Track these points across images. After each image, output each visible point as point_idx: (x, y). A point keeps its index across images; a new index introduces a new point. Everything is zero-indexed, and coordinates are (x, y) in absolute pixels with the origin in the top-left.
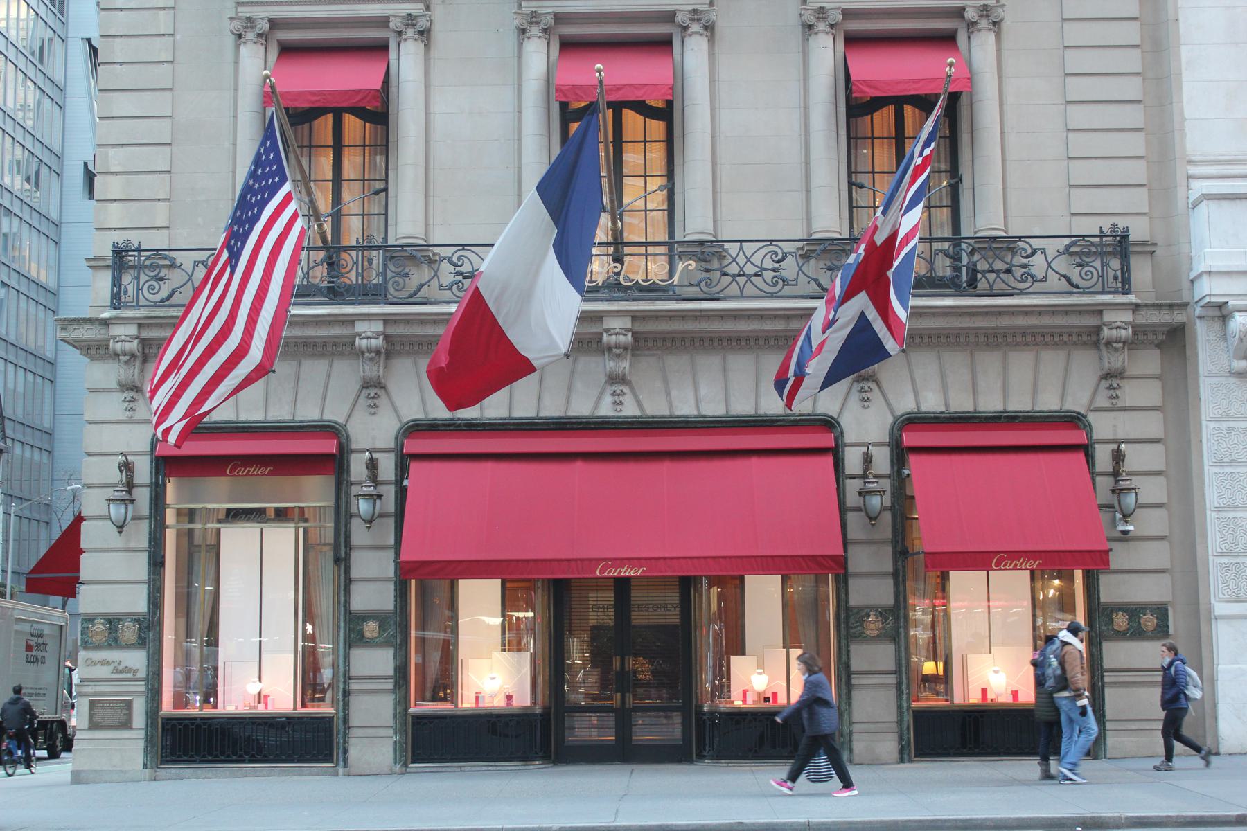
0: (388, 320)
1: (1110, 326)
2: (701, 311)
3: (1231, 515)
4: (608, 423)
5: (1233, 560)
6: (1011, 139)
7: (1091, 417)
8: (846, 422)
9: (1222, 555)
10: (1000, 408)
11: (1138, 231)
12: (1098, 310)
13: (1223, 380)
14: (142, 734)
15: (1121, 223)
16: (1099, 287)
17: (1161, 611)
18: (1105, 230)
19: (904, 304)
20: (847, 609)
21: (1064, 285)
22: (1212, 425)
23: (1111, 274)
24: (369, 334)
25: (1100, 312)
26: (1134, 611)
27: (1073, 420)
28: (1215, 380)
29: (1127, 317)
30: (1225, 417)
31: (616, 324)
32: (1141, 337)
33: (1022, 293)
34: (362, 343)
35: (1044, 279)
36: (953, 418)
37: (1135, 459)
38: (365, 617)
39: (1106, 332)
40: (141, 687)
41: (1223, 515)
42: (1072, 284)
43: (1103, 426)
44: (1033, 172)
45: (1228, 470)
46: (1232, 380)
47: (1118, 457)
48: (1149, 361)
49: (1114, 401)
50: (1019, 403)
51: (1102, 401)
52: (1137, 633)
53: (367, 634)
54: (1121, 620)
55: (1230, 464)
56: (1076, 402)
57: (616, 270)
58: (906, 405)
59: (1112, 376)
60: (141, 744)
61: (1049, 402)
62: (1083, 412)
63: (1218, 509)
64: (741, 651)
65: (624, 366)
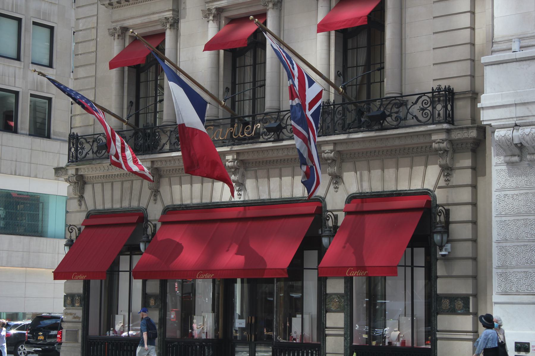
1: (434, 141)
2: (261, 148)
3: (504, 244)
4: (235, 204)
5: (504, 271)
7: (437, 192)
8: (328, 200)
9: (498, 267)
10: (394, 189)
11: (460, 85)
12: (429, 133)
14: (80, 344)
15: (444, 84)
16: (431, 121)
17: (465, 299)
18: (435, 89)
20: (146, 294)
21: (414, 121)
22: (497, 193)
23: (437, 112)
24: (438, 141)
25: (430, 135)
26: (452, 298)
29: (443, 136)
31: (229, 157)
35: (405, 119)
36: (373, 195)
37: (460, 214)
38: (151, 296)
39: (435, 145)
40: (80, 326)
41: (501, 244)
42: (419, 121)
43: (441, 197)
44: (419, 57)
45: (504, 219)
47: (447, 212)
49: (447, 183)
51: (442, 183)
52: (453, 311)
53: (151, 305)
54: (446, 303)
57: (232, 131)
58: (353, 189)
60: (79, 349)
62: (432, 189)
63: (498, 242)
64: (117, 314)
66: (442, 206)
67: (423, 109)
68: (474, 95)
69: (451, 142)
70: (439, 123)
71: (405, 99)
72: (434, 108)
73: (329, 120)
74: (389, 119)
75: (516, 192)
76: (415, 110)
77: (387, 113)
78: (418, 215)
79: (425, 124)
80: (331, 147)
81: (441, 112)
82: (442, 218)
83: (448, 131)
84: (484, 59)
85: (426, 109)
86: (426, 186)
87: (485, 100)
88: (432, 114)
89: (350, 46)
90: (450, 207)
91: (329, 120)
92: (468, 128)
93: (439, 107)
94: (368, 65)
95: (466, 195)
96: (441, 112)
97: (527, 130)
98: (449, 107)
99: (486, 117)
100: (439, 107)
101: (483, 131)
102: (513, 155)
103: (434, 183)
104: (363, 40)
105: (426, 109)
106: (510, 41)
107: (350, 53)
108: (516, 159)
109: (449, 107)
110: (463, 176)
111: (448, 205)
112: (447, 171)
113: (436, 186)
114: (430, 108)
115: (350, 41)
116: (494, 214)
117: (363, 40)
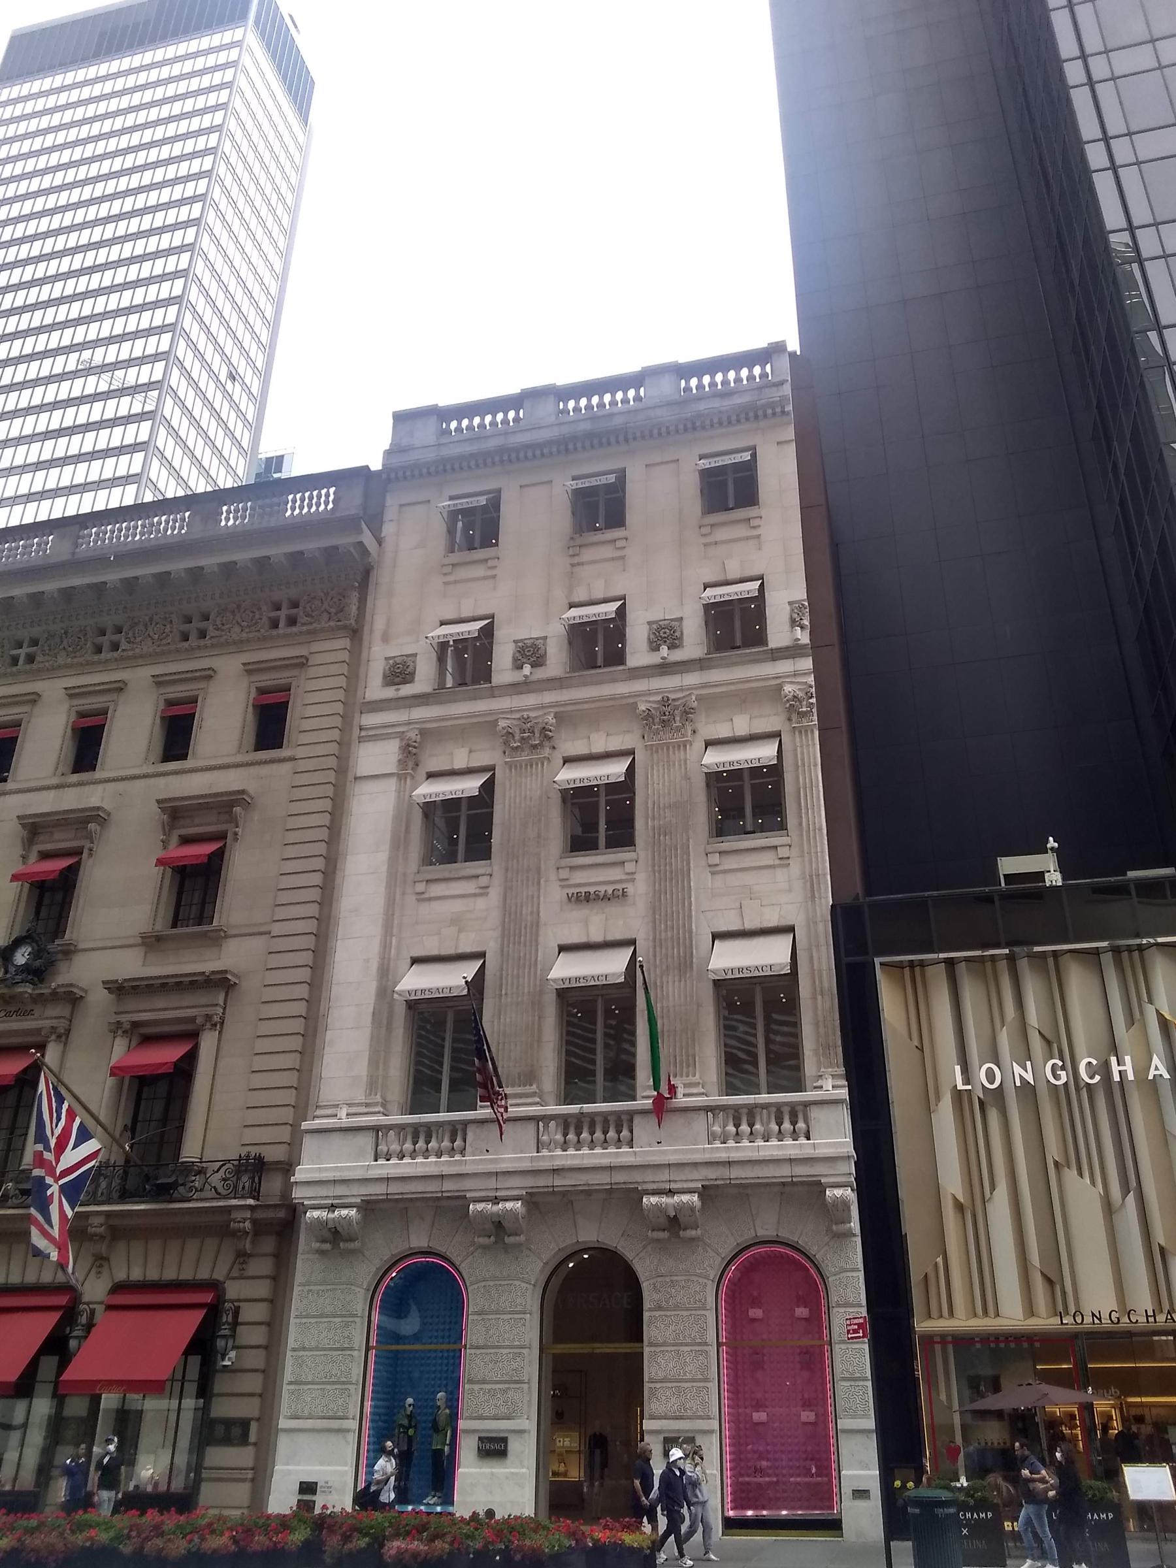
0: (108, 1214)
6: (217, 1098)
11: (273, 1154)
12: (229, 1210)
13: (311, 1256)
15: (254, 1151)
16: (232, 1195)
19: (73, 1209)
21: (215, 1195)
25: (230, 1212)
27: (214, 1286)
28: (306, 1256)
30: (308, 1283)
32: (260, 1228)
33: (189, 1200)
34: (91, 1230)
37: (252, 1313)
43: (233, 1290)
45: (304, 1320)
46: (317, 1256)
48: (268, 1245)
50: (186, 1275)
55: (307, 1317)
56: (219, 1275)
59: (242, 1257)
61: (204, 1274)
62: (221, 1279)
65: (103, 1248)
66: (232, 1301)
67: (225, 1180)
68: (287, 1167)
69: (254, 1222)
70: (243, 1197)
71: (204, 1165)
72: (239, 1179)
73: (104, 1185)
74: (181, 1189)
75: (322, 1288)
76: (215, 1180)
77: (180, 1182)
78: (198, 1316)
79: (225, 1197)
80: (101, 1220)
81: (247, 1185)
82: (230, 1319)
83: (250, 1207)
84: (305, 1125)
85: (228, 1179)
86: (215, 1276)
87: (302, 1173)
88: (235, 1187)
89: (144, 1096)
90: (241, 1304)
91: (104, 1185)
92: (275, 1206)
93: (245, 1178)
94: (164, 1120)
95: (262, 1289)
96: (247, 1185)
97: (344, 1212)
98: (257, 1180)
99: (298, 1194)
100: (245, 1178)
101: (294, 1212)
102: (324, 1241)
103: (225, 1272)
104: (162, 1088)
105: (228, 1179)
106: (337, 1106)
107: (143, 1103)
108: (327, 1246)
109: (257, 1180)
110: (262, 1266)
111: (239, 1300)
112: (242, 1257)
113: (228, 1277)
114: (234, 1179)
115: (145, 1089)
116: (292, 1315)
117: (162, 1088)
